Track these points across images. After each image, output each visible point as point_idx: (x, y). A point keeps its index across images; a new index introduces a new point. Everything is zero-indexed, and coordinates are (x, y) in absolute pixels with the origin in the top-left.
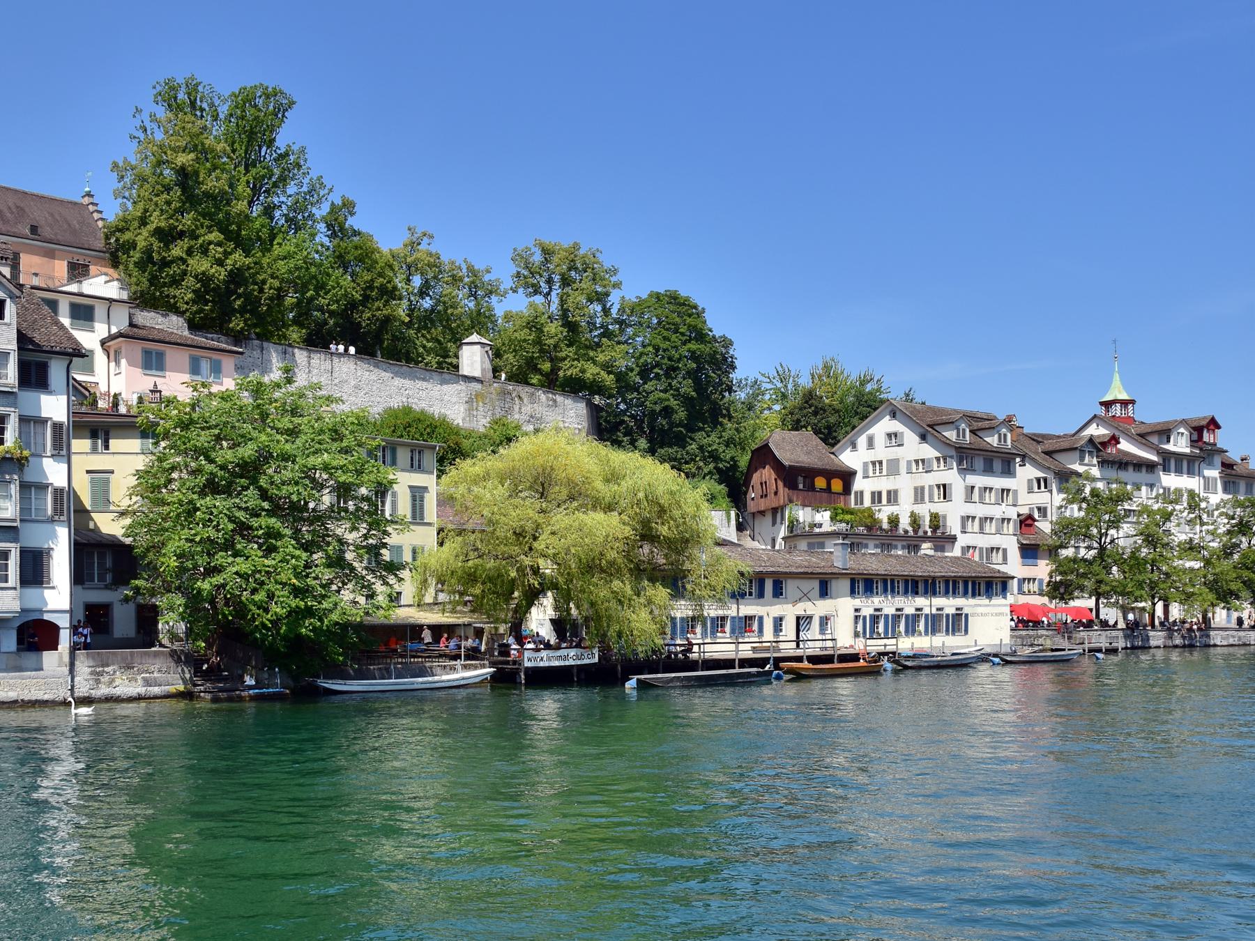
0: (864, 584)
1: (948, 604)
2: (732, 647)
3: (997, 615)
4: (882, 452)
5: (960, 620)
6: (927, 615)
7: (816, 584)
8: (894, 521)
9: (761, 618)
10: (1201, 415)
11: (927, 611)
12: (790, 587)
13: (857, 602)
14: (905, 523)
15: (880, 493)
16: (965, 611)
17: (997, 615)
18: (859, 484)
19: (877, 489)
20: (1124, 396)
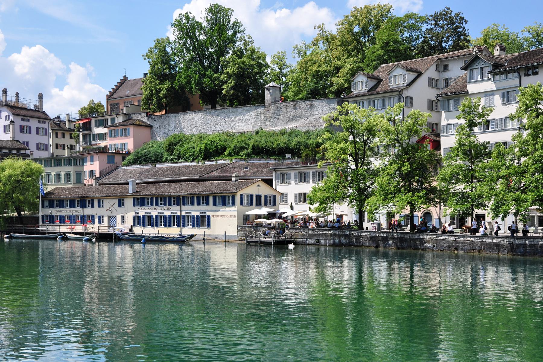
0: (141, 200)
3: (229, 216)
7: (116, 201)
11: (179, 213)
12: (107, 203)
13: (136, 208)
16: (208, 214)
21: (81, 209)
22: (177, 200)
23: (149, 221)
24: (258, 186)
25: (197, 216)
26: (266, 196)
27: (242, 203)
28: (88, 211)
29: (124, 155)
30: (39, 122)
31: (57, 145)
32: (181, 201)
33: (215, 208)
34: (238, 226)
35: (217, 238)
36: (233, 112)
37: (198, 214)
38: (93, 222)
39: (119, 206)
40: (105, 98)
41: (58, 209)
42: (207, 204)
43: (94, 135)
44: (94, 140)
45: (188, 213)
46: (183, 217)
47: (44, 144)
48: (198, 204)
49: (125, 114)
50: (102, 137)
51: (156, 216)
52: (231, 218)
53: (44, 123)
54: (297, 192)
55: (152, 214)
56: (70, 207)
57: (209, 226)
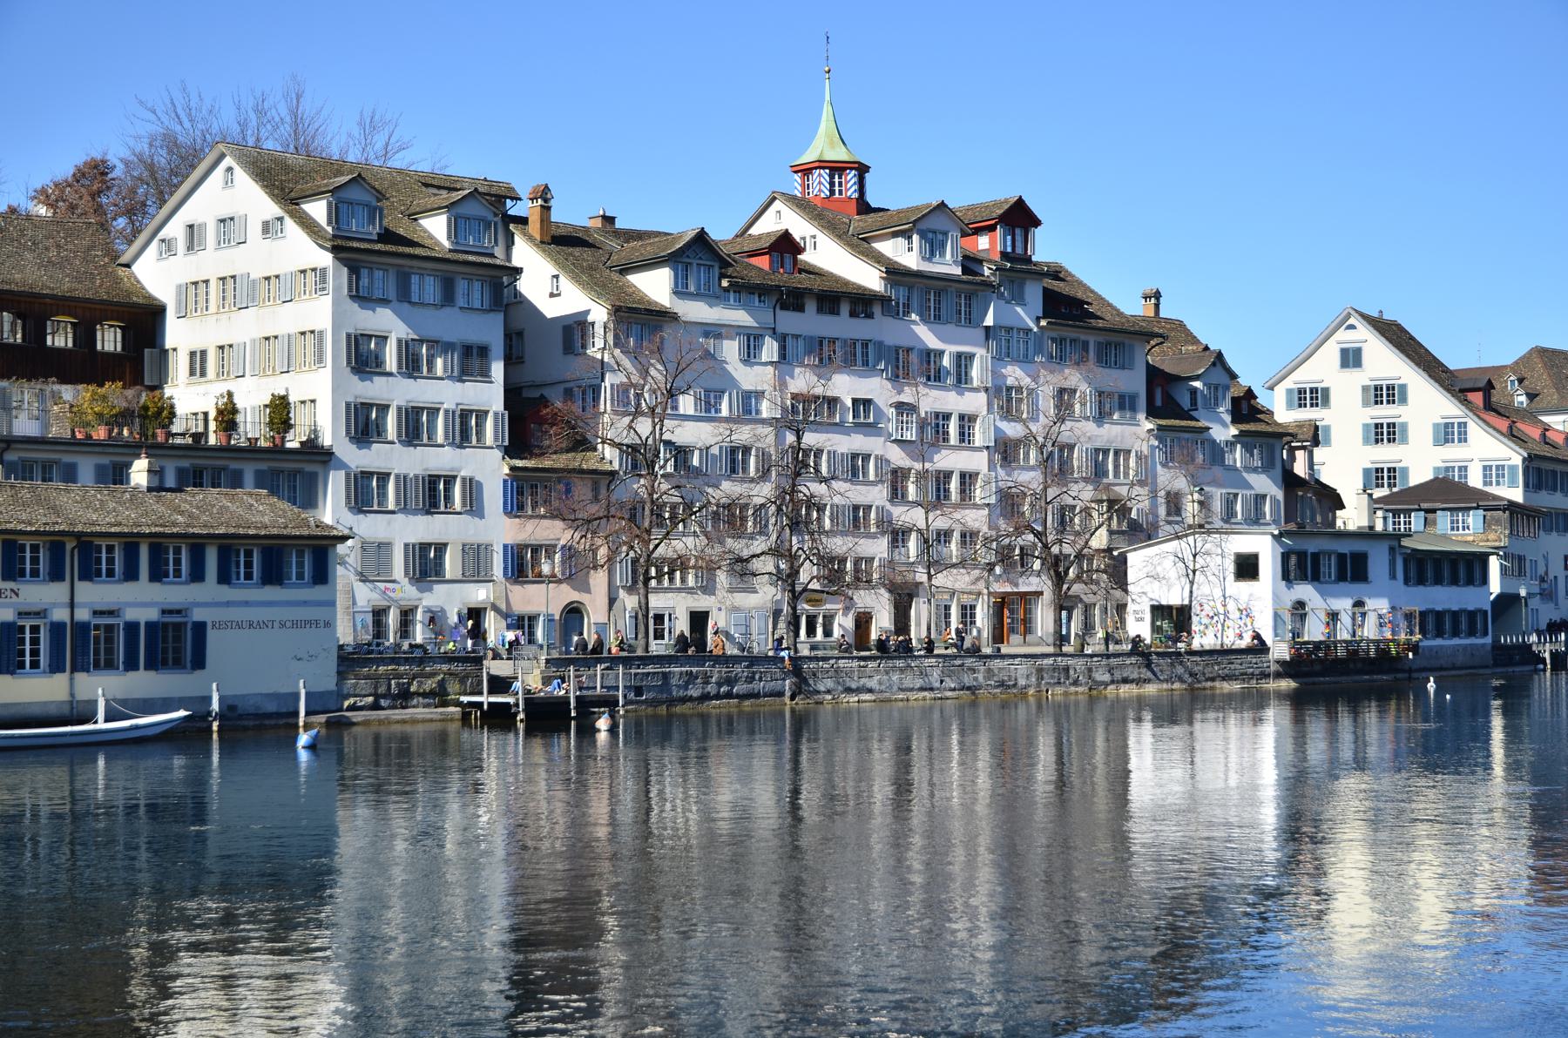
1: (140, 601)
3: (296, 624)
4: (211, 263)
5: (178, 639)
6: (57, 629)
8: (228, 416)
10: (1001, 196)
11: (60, 615)
14: (253, 427)
15: (204, 353)
16: (198, 615)
17: (296, 624)
18: (178, 335)
19: (197, 346)
20: (839, 154)
25: (151, 626)
32: (71, 562)
33: (226, 593)
37: (153, 615)
42: (197, 575)
45: (170, 612)
46: (81, 629)
48: (157, 575)
57: (199, 662)
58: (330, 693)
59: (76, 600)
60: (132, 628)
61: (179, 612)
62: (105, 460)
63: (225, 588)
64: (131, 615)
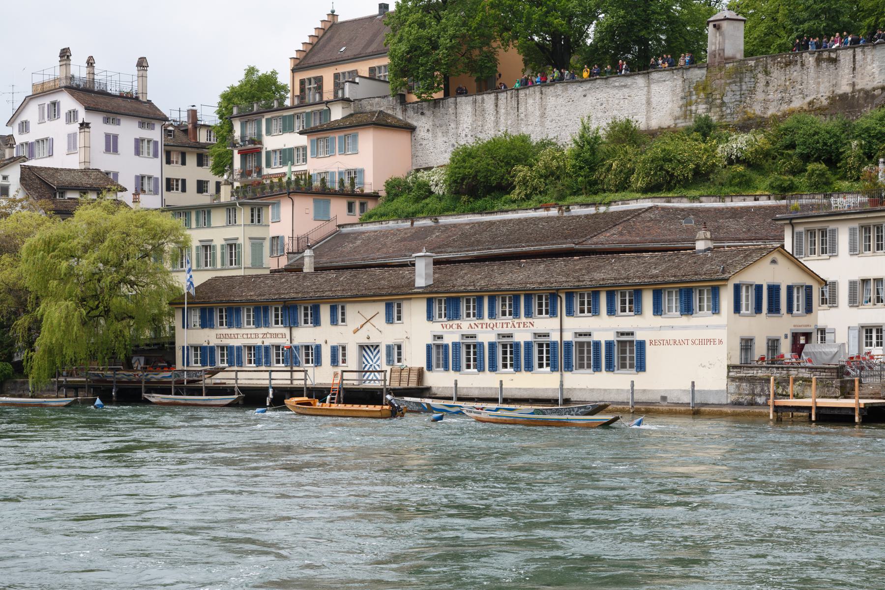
1: (603, 327)
2: (287, 375)
3: (702, 342)
7: (381, 308)
9: (318, 348)
11: (555, 337)
13: (436, 327)
16: (638, 337)
17: (702, 342)
21: (286, 331)
22: (549, 300)
23: (474, 355)
24: (774, 262)
25: (609, 344)
26: (790, 289)
27: (737, 309)
28: (304, 335)
29: (351, 200)
30: (142, 125)
31: (168, 180)
33: (659, 321)
34: (730, 367)
35: (664, 398)
36: (625, 86)
37: (612, 337)
38: (318, 362)
39: (389, 320)
40: (289, 65)
41: (225, 331)
43: (268, 153)
44: (268, 165)
46: (568, 345)
47: (149, 178)
48: (611, 311)
49: (348, 100)
50: (287, 156)
51: (492, 346)
52: (710, 347)
53: (151, 127)
54: (857, 277)
55: (480, 339)
56: (258, 325)
57: (641, 367)
58: (722, 391)
59: (564, 327)
60: (597, 344)
61: (628, 334)
62: (856, 225)
63: (658, 318)
64: (595, 337)
